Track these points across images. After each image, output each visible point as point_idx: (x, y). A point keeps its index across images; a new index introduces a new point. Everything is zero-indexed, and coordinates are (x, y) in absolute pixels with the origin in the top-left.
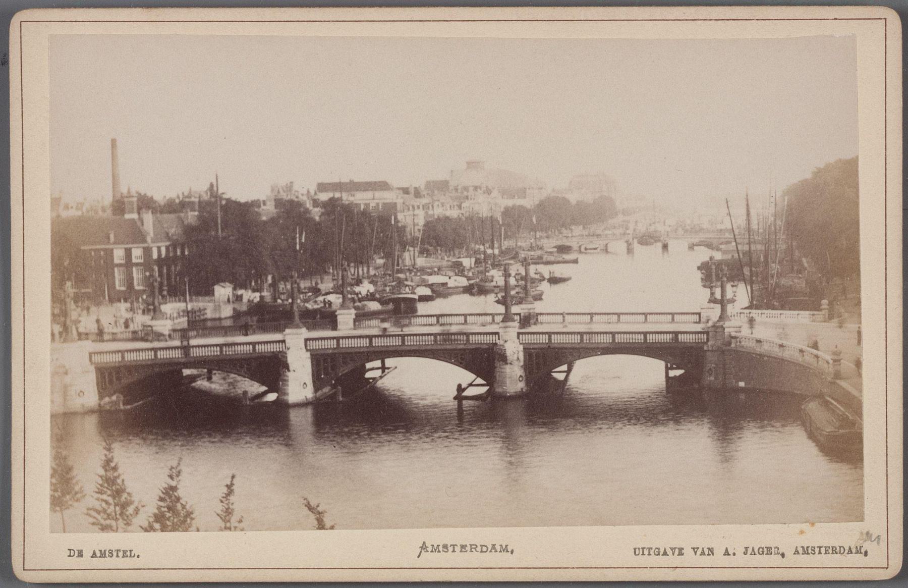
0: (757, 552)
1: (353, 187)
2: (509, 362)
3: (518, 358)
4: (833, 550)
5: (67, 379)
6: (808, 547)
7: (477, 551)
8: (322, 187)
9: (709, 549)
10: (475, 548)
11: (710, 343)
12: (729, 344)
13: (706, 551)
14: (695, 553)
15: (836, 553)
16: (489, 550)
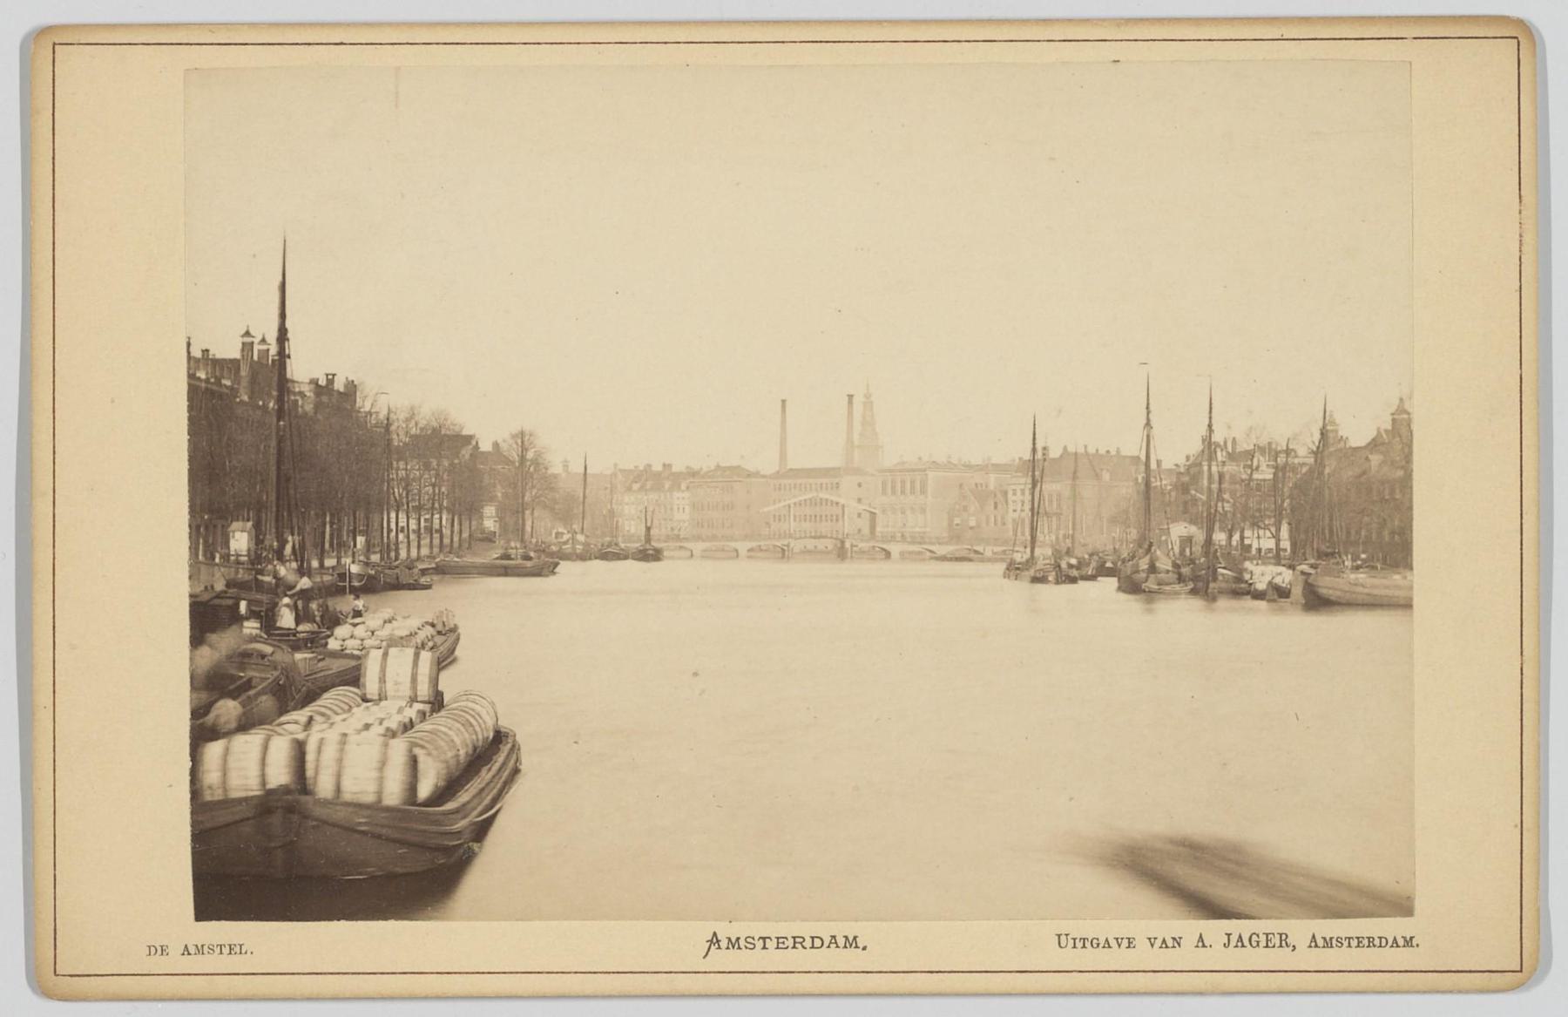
0: (1246, 942)
4: (1369, 942)
6: (1331, 939)
7: (805, 948)
9: (1174, 939)
10: (801, 943)
13: (1170, 943)
14: (1152, 945)
15: (1374, 946)
16: (826, 944)
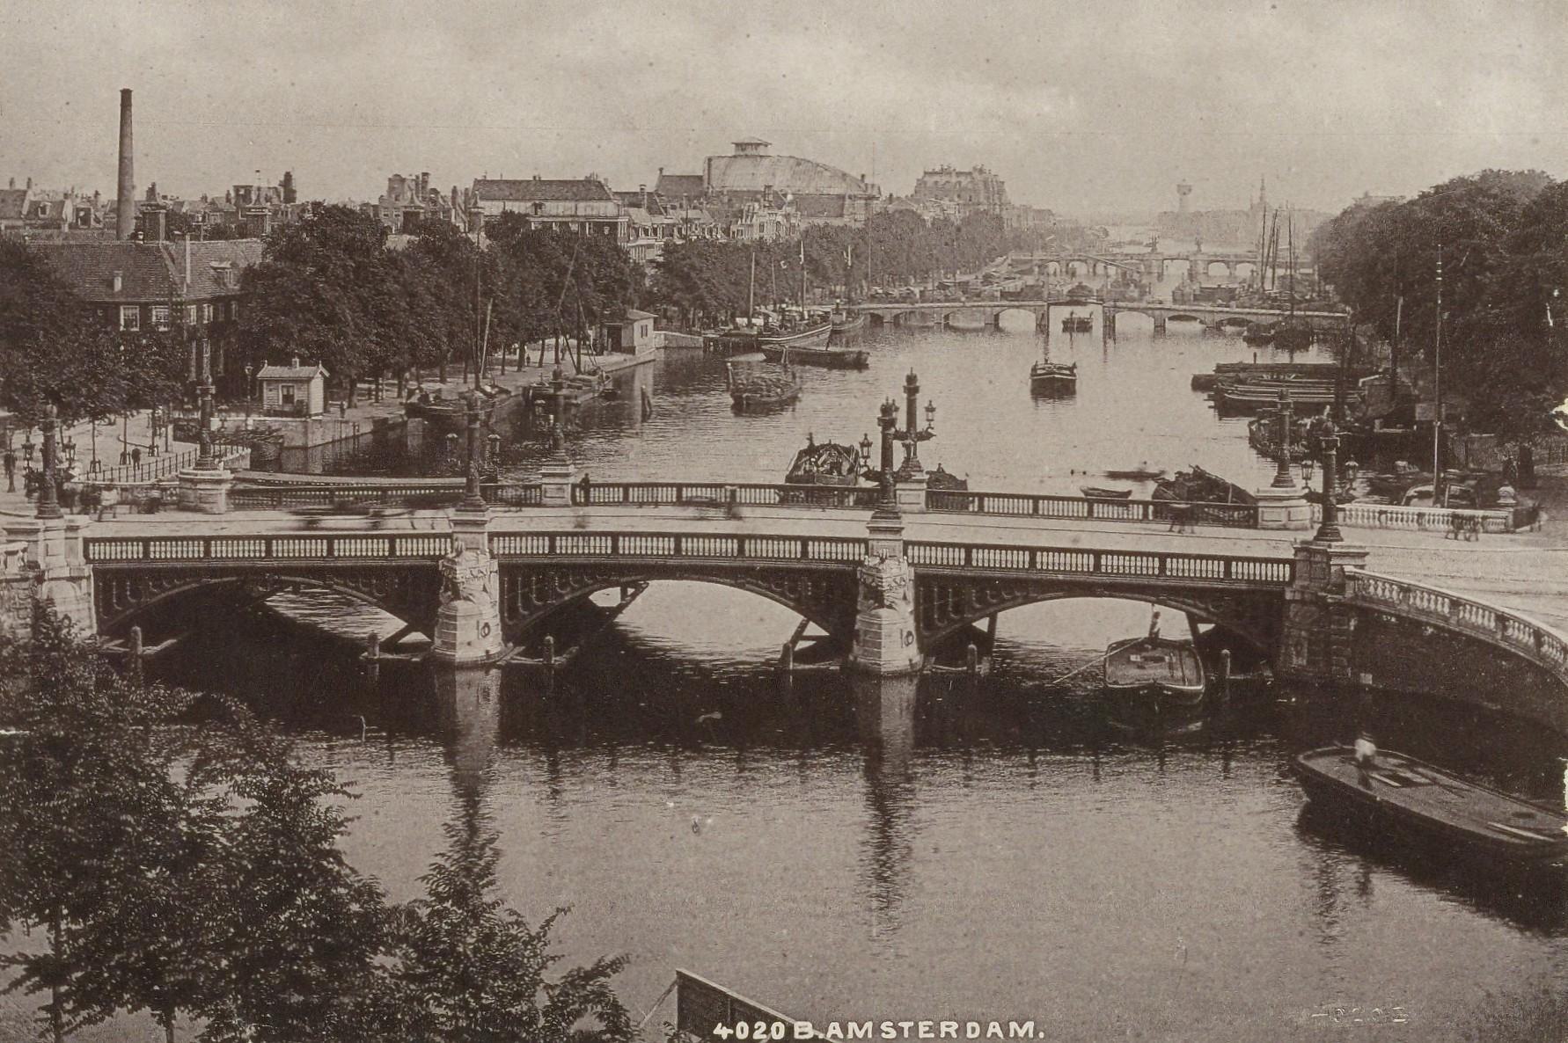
1: (538, 189)
2: (887, 603)
3: (905, 598)
5: (44, 590)
8: (487, 188)
11: (1298, 583)
12: (1341, 588)
